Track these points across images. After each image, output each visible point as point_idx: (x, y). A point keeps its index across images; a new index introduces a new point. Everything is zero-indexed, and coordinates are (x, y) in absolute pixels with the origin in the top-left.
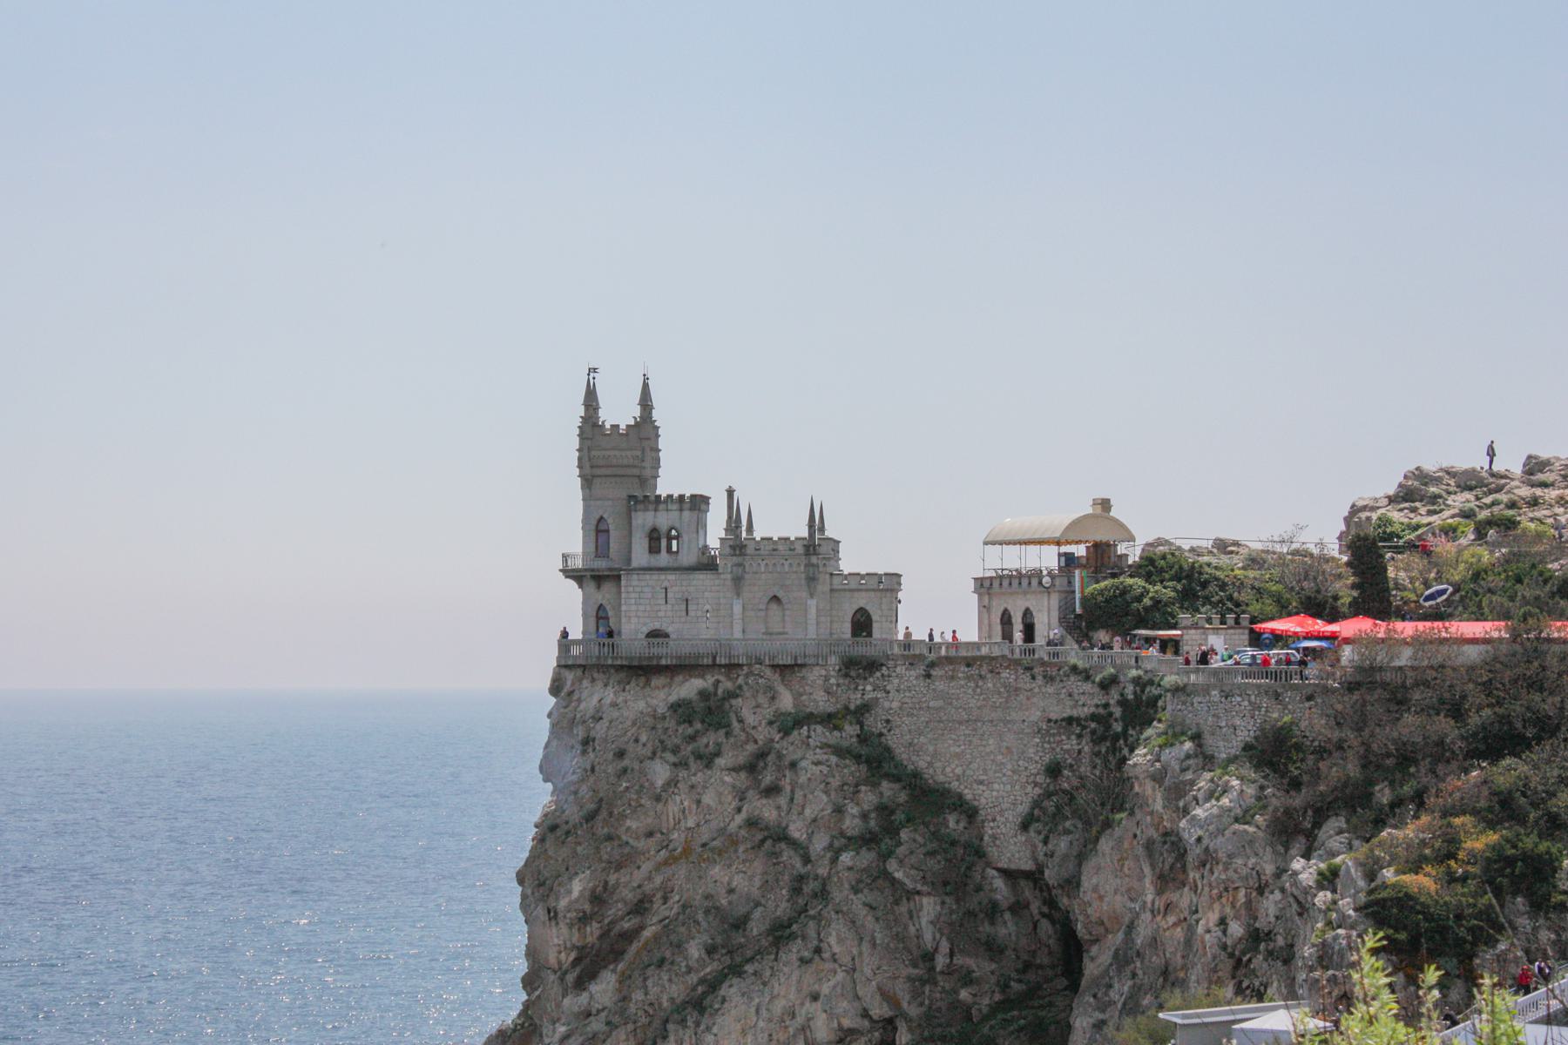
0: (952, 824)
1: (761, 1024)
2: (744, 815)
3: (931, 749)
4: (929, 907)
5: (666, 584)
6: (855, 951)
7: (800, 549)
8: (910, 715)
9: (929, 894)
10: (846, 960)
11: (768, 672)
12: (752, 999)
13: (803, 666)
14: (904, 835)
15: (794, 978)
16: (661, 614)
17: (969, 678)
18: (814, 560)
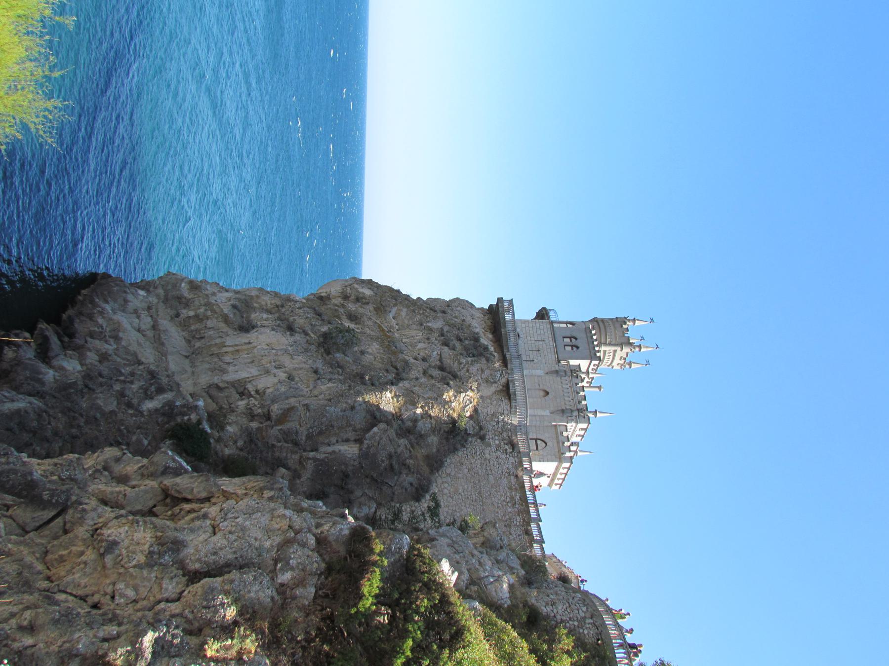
0: (410, 479)
1: (274, 351)
2: (412, 360)
3: (460, 475)
4: (350, 450)
5: (547, 341)
6: (320, 397)
7: (579, 407)
8: (482, 465)
9: (360, 450)
10: (316, 392)
11: (504, 380)
12: (292, 346)
13: (510, 399)
14: (403, 441)
15: (304, 365)
16: (529, 338)
17: (512, 498)
18: (576, 413)
